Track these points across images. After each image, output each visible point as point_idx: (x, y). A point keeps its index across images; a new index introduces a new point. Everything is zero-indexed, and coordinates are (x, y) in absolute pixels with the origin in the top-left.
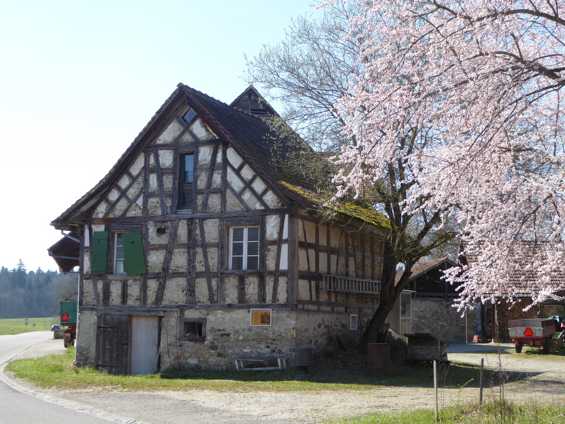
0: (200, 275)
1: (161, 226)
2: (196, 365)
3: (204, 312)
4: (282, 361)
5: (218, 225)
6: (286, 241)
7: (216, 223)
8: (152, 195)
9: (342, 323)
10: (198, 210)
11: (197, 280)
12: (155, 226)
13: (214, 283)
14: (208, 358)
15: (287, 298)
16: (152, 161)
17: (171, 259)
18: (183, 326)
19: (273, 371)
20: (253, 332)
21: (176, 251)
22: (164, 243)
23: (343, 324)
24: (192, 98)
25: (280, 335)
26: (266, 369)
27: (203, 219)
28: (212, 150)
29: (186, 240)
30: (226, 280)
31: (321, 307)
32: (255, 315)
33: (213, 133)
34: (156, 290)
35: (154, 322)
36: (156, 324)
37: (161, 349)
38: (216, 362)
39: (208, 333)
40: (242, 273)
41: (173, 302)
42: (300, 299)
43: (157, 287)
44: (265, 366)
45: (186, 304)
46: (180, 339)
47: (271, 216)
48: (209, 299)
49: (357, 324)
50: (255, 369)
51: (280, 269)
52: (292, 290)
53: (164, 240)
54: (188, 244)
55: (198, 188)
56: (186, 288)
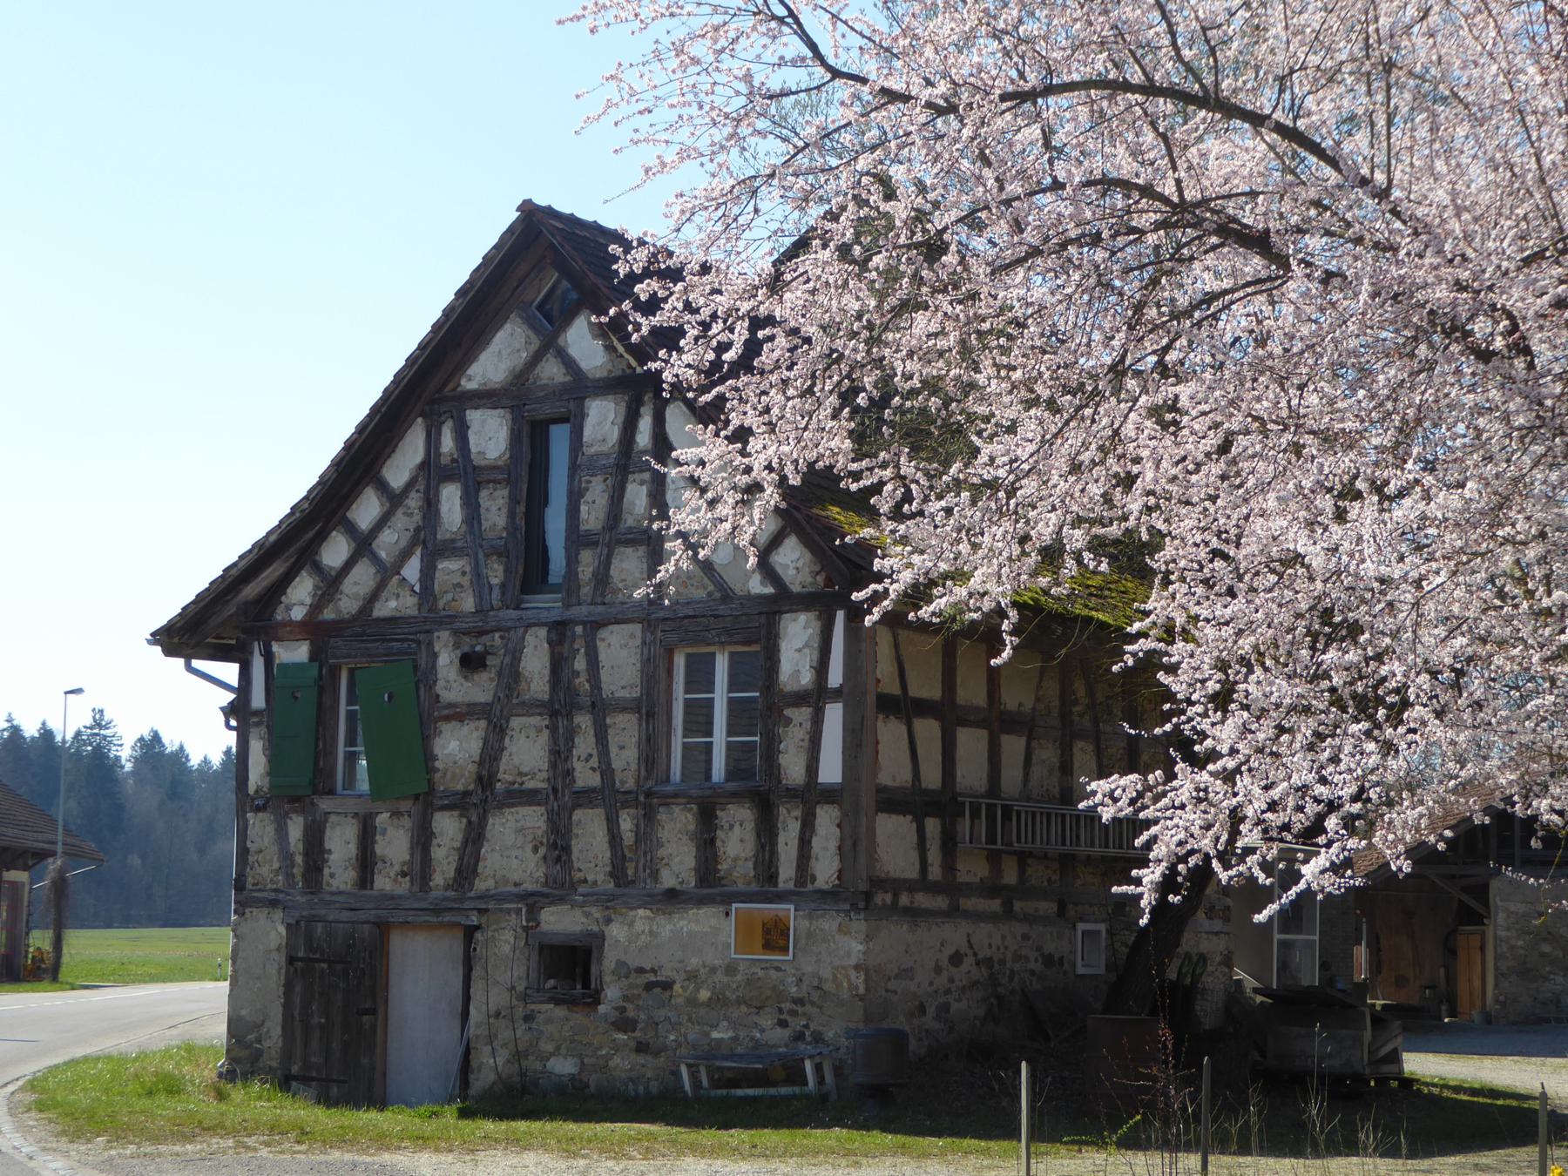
0: (585, 797)
1: (473, 646)
2: (572, 1077)
3: (596, 912)
4: (818, 1068)
5: (638, 642)
6: (837, 694)
7: (632, 636)
8: (448, 549)
9: (1046, 951)
10: (583, 598)
11: (578, 815)
12: (456, 646)
13: (626, 824)
14: (608, 1057)
15: (840, 871)
16: (447, 443)
17: (503, 749)
18: (535, 956)
19: (794, 1097)
20: (739, 977)
21: (515, 722)
22: (483, 700)
23: (1051, 956)
24: (562, 247)
25: (818, 988)
26: (772, 1091)
27: (595, 626)
28: (622, 409)
29: (547, 688)
30: (662, 816)
31: (962, 901)
32: (743, 928)
33: (626, 356)
34: (457, 844)
35: (452, 944)
36: (458, 949)
37: (472, 1030)
38: (631, 1070)
39: (607, 978)
40: (708, 792)
41: (505, 881)
42: (883, 875)
43: (460, 837)
44: (774, 1084)
45: (545, 890)
46: (525, 998)
47: (793, 615)
48: (611, 874)
49: (1104, 957)
50: (740, 1092)
51: (820, 780)
52: (854, 845)
53: (480, 689)
54: (551, 700)
55: (582, 528)
56: (545, 841)
